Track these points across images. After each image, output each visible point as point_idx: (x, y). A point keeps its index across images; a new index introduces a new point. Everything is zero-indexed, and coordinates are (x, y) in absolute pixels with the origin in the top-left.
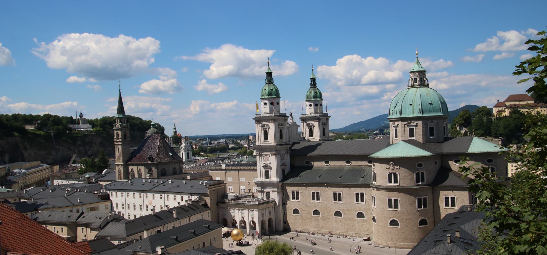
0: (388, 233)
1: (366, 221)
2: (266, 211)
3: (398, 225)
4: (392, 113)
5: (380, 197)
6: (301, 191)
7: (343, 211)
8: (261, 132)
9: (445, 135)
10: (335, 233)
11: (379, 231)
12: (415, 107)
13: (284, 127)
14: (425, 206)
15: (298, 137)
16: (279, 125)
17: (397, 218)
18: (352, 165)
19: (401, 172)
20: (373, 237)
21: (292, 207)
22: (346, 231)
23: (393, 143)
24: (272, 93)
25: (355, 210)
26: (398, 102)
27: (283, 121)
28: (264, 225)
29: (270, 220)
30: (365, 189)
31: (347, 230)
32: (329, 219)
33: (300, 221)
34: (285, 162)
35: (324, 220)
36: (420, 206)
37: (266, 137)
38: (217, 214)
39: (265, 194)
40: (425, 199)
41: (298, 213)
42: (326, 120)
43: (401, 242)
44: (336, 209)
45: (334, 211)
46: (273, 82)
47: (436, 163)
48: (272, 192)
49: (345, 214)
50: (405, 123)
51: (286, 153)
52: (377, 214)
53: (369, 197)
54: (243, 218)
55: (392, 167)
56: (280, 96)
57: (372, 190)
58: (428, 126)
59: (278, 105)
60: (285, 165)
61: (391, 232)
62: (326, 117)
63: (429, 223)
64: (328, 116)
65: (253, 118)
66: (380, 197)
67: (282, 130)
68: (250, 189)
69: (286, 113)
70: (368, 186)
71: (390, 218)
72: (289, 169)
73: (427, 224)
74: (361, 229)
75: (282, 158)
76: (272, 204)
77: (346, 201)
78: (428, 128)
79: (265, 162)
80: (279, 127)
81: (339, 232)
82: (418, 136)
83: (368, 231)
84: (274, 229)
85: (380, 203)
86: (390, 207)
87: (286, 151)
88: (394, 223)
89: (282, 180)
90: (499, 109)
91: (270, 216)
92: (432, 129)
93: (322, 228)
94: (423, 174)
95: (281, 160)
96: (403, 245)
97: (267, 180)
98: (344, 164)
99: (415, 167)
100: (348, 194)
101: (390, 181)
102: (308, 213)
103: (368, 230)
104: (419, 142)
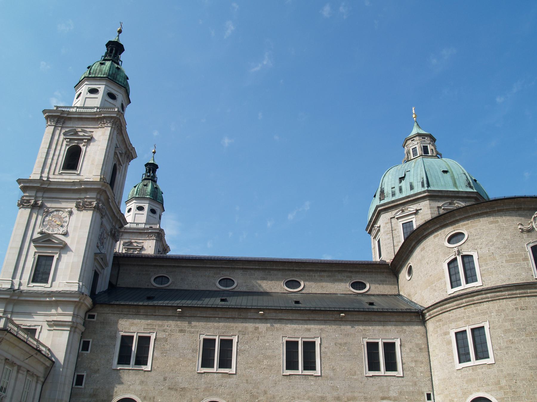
5: (512, 320)
6: (161, 335)
8: (59, 148)
12: (456, 176)
18: (303, 292)
24: (118, 77)
30: (399, 328)
50: (440, 204)
52: (503, 383)
53: (413, 355)
66: (512, 320)
77: (333, 370)
85: (516, 339)
97: (38, 287)
98: (281, 288)
100: (341, 344)
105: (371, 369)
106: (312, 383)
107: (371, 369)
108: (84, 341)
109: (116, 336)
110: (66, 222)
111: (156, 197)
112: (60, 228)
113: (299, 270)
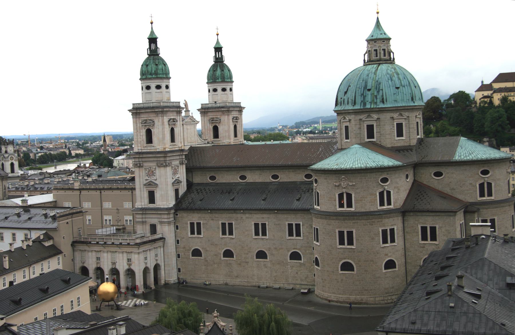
0: (338, 282)
1: (304, 264)
2: (150, 254)
3: (353, 270)
4: (341, 102)
5: (325, 229)
6: (205, 222)
7: (269, 250)
9: (418, 135)
10: (258, 283)
11: (325, 280)
13: (177, 123)
14: (393, 240)
15: (196, 139)
16: (169, 121)
17: (351, 259)
18: (281, 181)
19: (358, 191)
20: (316, 288)
21: (191, 247)
22: (274, 281)
23: (343, 147)
24: (158, 71)
25: (287, 249)
26: (350, 86)
27: (176, 115)
28: (148, 274)
29: (157, 267)
31: (275, 278)
32: (247, 263)
33: (204, 267)
34: (178, 178)
35: (240, 264)
36: (385, 241)
37: (149, 139)
38: (72, 261)
39: (148, 228)
40: (392, 230)
41: (201, 256)
42: (237, 113)
43: (358, 295)
44: (258, 248)
45: (256, 250)
46: (160, 54)
47: (407, 177)
48: (158, 223)
49: (272, 254)
51: (180, 164)
52: (321, 254)
53: (308, 229)
54: (114, 263)
55: (344, 183)
56: (171, 75)
57: (314, 218)
58: (394, 122)
59: (167, 90)
60: (178, 183)
61: (342, 280)
62: (240, 109)
63: (398, 265)
64: (240, 107)
65: (128, 110)
67: (175, 129)
68: (119, 219)
69: (179, 102)
70: (307, 211)
71: (341, 259)
72: (186, 189)
73: (395, 268)
74: (296, 277)
75: (175, 173)
76: (160, 243)
77: (274, 236)
78: (394, 124)
79: (148, 178)
80: (170, 123)
81: (263, 283)
82: (380, 137)
83: (307, 280)
84: (163, 282)
86: (342, 242)
87: (180, 161)
88: (347, 267)
89: (174, 205)
90: (483, 95)
91: (157, 260)
92: (400, 126)
93: (237, 277)
94: (389, 193)
95: (173, 174)
96: (360, 299)
97: (152, 206)
98: (269, 179)
99: (379, 183)
101: (341, 205)
102: (216, 255)
103: (306, 278)
104: (382, 146)
105: (289, 235)
106: (265, 242)
107: (289, 235)
108: (176, 226)
109: (187, 223)
110: (155, 173)
111: (224, 78)
112: (153, 176)
113: (278, 169)
